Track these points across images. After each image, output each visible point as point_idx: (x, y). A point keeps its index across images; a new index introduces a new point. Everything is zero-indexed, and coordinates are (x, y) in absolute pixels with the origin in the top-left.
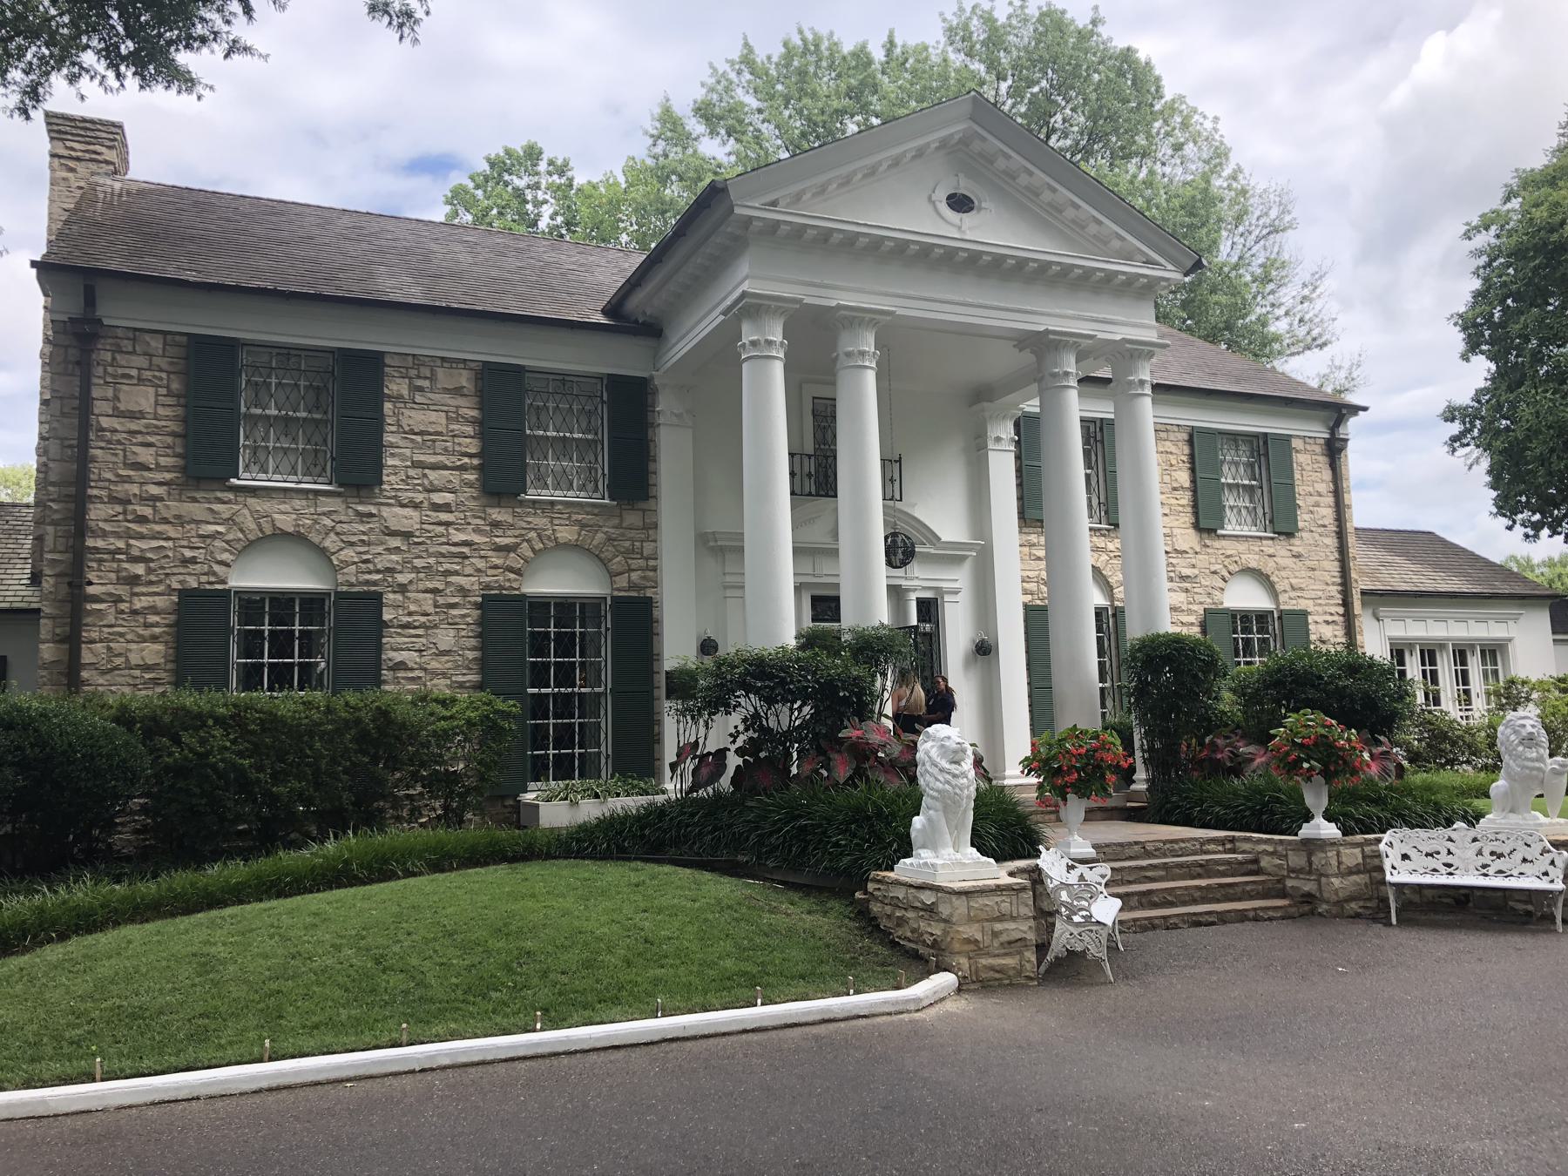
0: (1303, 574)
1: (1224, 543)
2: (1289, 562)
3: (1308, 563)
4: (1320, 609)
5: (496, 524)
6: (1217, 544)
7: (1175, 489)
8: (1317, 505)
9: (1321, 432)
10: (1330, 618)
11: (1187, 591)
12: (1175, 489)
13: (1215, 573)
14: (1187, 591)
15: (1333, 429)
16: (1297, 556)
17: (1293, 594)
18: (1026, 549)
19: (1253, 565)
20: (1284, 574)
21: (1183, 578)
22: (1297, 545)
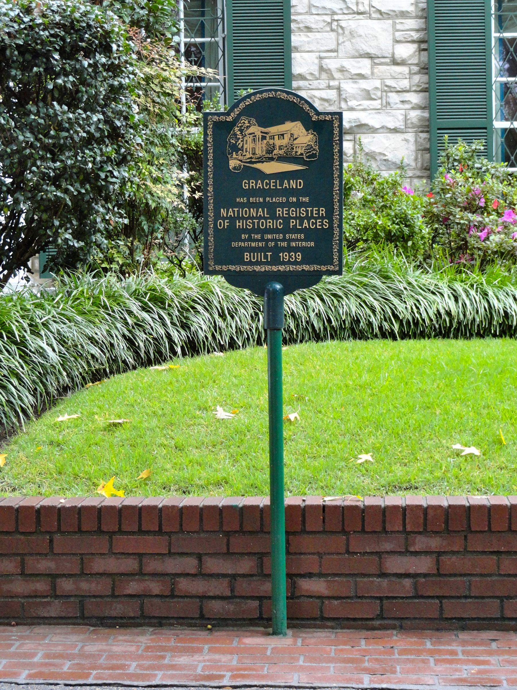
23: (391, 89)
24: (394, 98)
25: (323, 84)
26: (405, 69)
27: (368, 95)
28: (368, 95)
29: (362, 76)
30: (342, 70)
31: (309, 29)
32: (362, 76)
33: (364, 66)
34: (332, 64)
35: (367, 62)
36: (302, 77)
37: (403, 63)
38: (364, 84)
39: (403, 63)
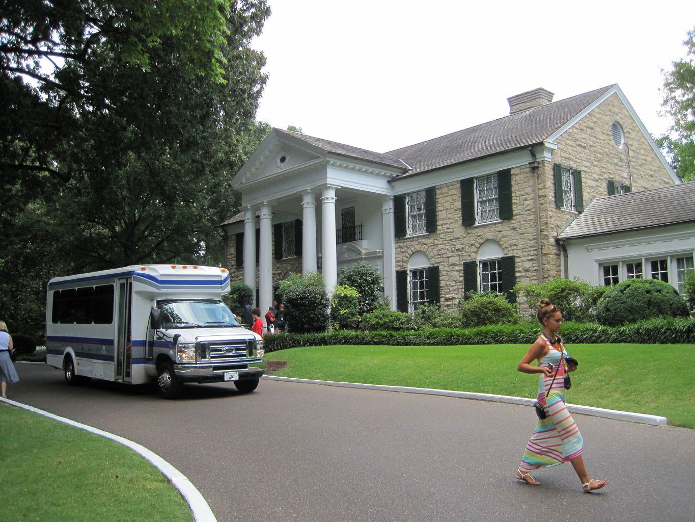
0: (518, 237)
1: (477, 230)
2: (510, 233)
3: (520, 231)
4: (525, 254)
5: (278, 268)
6: (474, 231)
7: (456, 210)
8: (526, 200)
9: (526, 160)
10: (530, 258)
11: (459, 256)
12: (456, 210)
13: (472, 245)
14: (459, 256)
15: (533, 155)
16: (514, 229)
17: (510, 249)
18: (399, 250)
19: (491, 238)
20: (506, 239)
21: (458, 250)
22: (514, 223)
23: (459, 288)
24: (460, 290)
25: (446, 288)
26: (461, 283)
27: (455, 290)
28: (455, 290)
29: (454, 286)
30: (450, 284)
31: (444, 276)
32: (454, 286)
33: (454, 283)
34: (448, 283)
35: (454, 282)
36: (442, 287)
37: (461, 282)
38: (454, 288)
39: (461, 282)
